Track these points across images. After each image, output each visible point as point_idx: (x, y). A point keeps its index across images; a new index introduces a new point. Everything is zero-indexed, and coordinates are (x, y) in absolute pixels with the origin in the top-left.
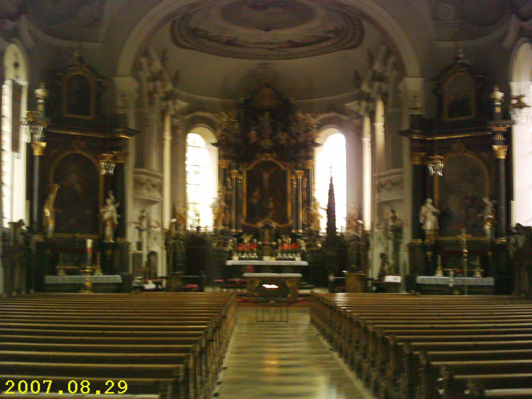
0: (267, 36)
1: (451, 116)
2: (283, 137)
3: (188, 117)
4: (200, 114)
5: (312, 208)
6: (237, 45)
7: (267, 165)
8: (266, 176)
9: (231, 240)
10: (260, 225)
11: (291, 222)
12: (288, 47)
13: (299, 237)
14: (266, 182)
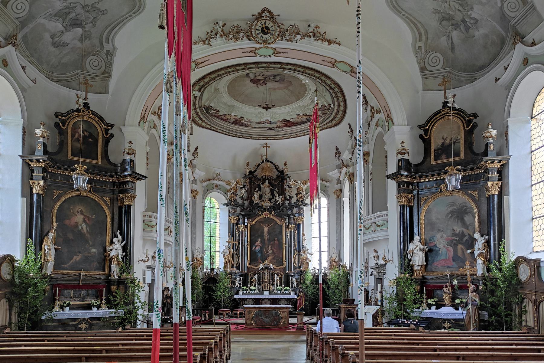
0: (267, 115)
1: (437, 158)
2: (280, 200)
3: (205, 184)
4: (215, 182)
5: (301, 253)
6: (242, 125)
7: (267, 221)
8: (266, 229)
9: (238, 279)
10: (261, 266)
11: (286, 264)
12: (283, 126)
13: (292, 276)
14: (266, 233)
